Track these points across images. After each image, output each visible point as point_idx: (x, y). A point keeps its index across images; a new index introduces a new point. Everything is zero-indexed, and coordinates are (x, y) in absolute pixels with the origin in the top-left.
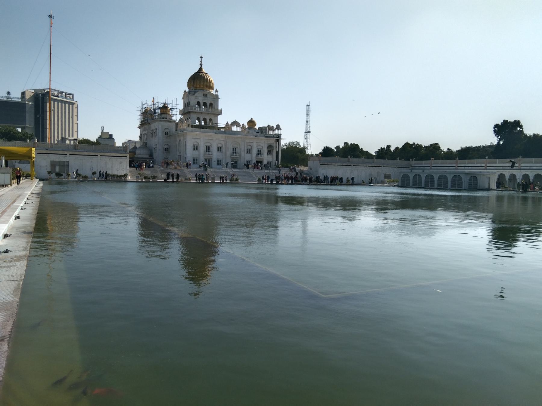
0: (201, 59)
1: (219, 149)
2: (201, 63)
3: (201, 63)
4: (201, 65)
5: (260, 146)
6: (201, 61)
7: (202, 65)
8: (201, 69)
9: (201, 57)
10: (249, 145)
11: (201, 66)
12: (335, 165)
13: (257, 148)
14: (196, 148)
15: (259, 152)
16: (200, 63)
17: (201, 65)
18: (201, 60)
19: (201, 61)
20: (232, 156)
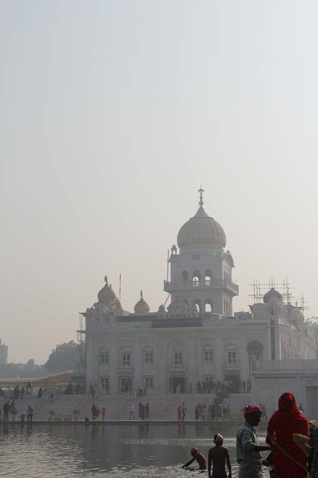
0: (201, 194)
1: (149, 358)
2: (201, 200)
3: (201, 200)
4: (201, 203)
5: (231, 344)
6: (201, 198)
7: (203, 203)
8: (201, 211)
9: (201, 190)
10: (208, 345)
11: (201, 206)
12: (295, 377)
13: (227, 350)
14: (128, 362)
15: (232, 356)
16: (199, 200)
17: (201, 203)
18: (201, 194)
19: (201, 198)
20: (170, 370)
